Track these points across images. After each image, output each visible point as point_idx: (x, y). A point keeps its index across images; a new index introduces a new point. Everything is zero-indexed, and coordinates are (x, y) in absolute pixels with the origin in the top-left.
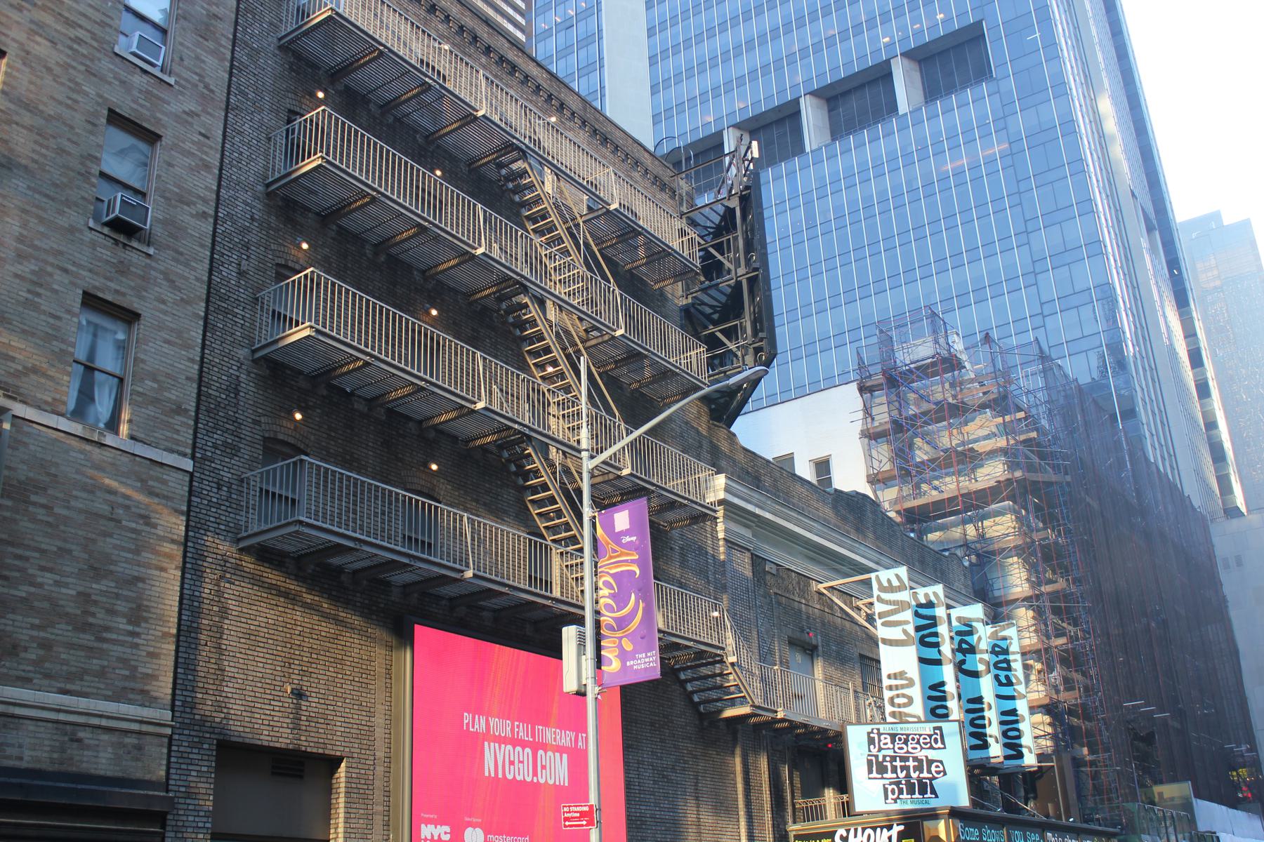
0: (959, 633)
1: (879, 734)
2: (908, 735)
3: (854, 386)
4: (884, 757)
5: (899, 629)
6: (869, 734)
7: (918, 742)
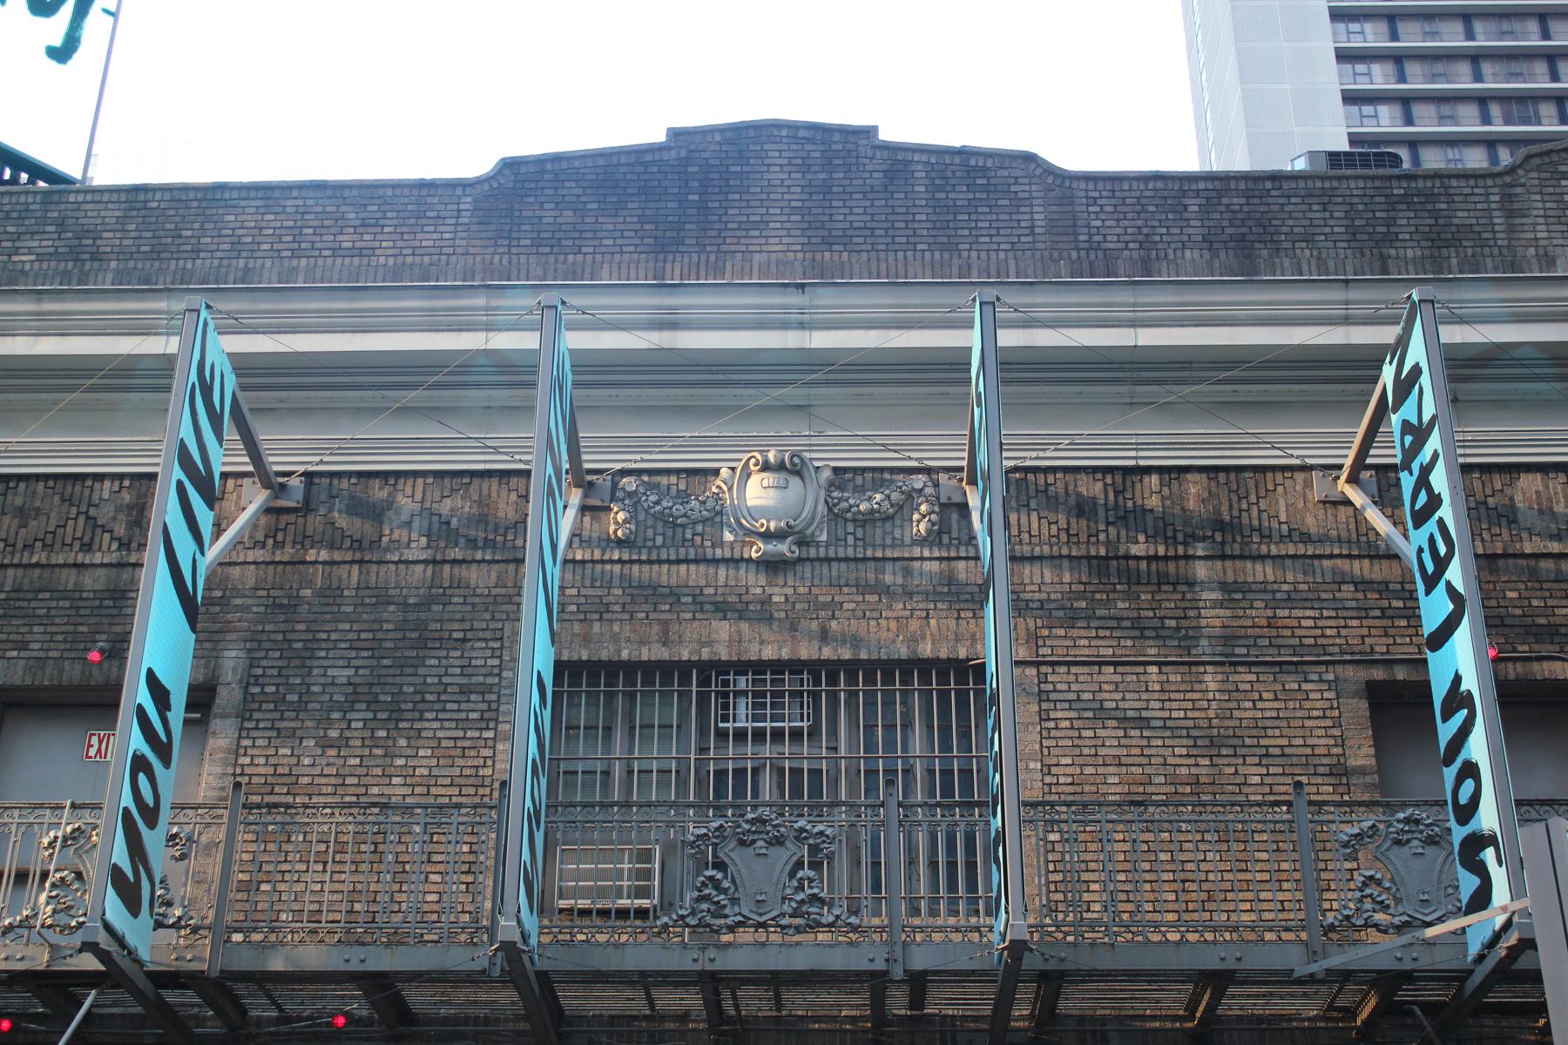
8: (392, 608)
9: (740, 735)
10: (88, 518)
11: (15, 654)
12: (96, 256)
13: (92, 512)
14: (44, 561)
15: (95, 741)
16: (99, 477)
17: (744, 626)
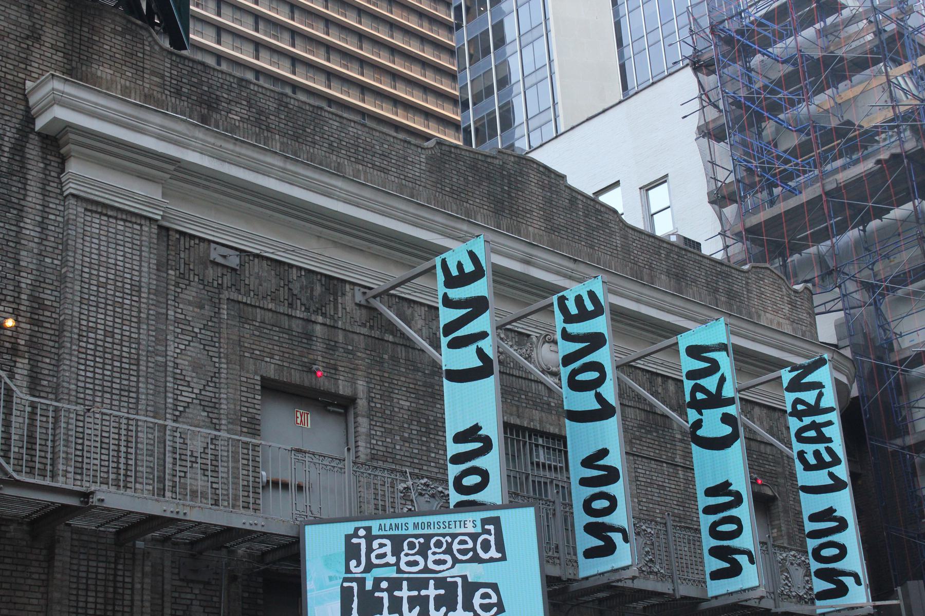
0: (692, 375)
1: (370, 538)
2: (428, 537)
3: (689, 71)
4: (377, 581)
5: (472, 348)
6: (348, 538)
7: (449, 551)
8: (420, 374)
9: (544, 465)
10: (290, 289)
11: (268, 359)
12: (268, 129)
13: (291, 286)
14: (273, 309)
15: (299, 415)
16: (291, 266)
17: (543, 414)
